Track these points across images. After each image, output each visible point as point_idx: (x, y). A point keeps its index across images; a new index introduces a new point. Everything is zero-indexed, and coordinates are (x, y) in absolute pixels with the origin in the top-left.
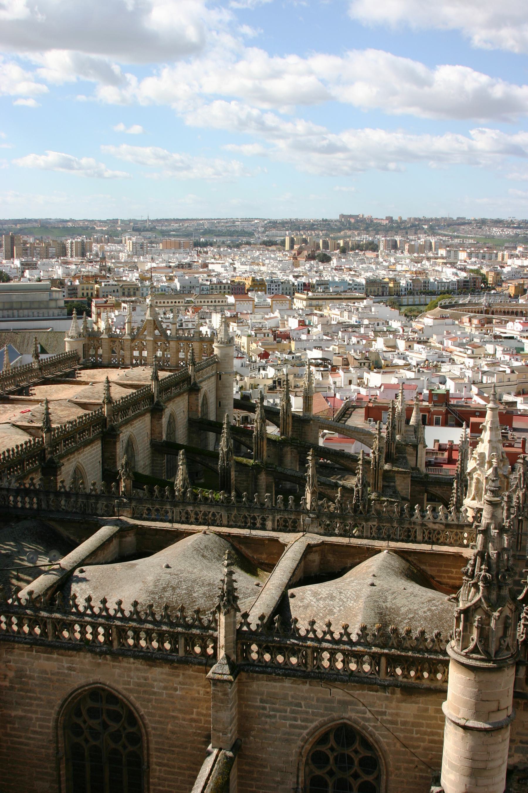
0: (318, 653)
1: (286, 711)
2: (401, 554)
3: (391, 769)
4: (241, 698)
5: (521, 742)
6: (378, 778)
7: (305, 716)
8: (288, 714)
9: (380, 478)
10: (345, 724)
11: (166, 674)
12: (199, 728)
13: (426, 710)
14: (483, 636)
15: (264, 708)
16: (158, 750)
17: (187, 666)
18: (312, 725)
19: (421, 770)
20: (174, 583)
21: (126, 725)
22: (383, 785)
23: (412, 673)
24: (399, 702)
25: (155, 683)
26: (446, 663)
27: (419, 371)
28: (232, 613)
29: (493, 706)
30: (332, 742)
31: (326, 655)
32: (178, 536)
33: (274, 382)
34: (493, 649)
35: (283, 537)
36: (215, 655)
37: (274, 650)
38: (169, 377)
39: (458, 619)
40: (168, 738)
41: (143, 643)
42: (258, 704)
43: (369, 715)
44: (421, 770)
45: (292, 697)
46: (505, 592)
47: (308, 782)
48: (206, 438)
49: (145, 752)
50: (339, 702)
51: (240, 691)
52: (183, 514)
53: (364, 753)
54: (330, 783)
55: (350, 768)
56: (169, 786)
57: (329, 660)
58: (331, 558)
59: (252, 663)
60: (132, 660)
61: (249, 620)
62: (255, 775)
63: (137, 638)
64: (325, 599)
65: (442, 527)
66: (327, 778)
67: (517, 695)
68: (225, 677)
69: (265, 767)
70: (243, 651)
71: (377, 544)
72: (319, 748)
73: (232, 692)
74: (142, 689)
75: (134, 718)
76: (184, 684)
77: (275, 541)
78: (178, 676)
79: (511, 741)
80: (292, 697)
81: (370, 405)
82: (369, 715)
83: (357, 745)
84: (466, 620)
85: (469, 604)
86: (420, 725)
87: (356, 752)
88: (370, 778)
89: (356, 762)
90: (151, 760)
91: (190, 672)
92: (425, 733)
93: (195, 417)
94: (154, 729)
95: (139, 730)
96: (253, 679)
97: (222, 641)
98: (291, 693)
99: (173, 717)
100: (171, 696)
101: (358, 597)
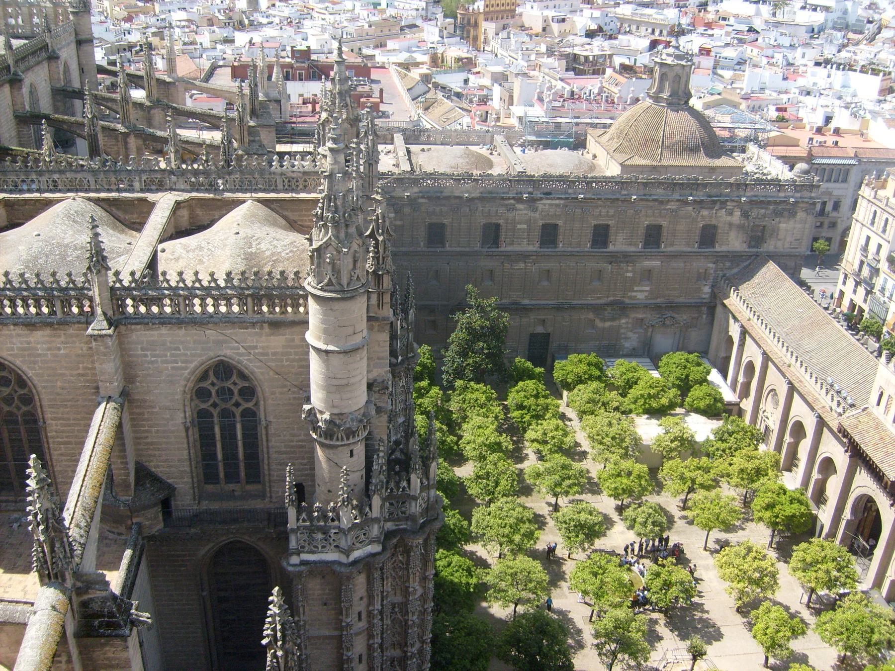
0: (189, 300)
1: (166, 356)
2: (265, 202)
3: (267, 394)
4: (122, 349)
5: (378, 358)
6: (257, 404)
7: (183, 358)
8: (169, 358)
9: (246, 133)
10: (222, 362)
11: (47, 336)
12: (87, 381)
13: (293, 340)
14: (336, 271)
15: (146, 356)
16: (51, 406)
17: (66, 327)
18: (192, 366)
19: (294, 393)
20: (47, 250)
21: (17, 388)
22: (262, 408)
23: (277, 309)
24: (267, 336)
25: (39, 346)
26: (305, 298)
27: (281, 28)
28: (103, 271)
29: (350, 330)
30: (212, 378)
31: (197, 301)
32: (49, 203)
33: (141, 46)
34: (345, 281)
35: (151, 197)
36: (93, 313)
37: (149, 302)
38: (25, 45)
39: (312, 257)
40: (59, 394)
41: (20, 310)
42: (140, 352)
43: (242, 350)
44: (294, 393)
45: (171, 343)
46: (352, 230)
47: (195, 416)
48: (73, 105)
49: (39, 410)
50: (214, 342)
51: (121, 343)
52: (50, 182)
53: (242, 384)
54: (215, 412)
55: (231, 398)
56: (67, 437)
57: (201, 305)
58: (199, 212)
59: (128, 317)
60: (12, 327)
61: (121, 277)
62: (146, 416)
63: (14, 305)
64: (194, 251)
65: (300, 175)
66: (212, 409)
67: (370, 319)
68: (104, 332)
69: (154, 407)
70: (119, 306)
71: (240, 195)
72: (201, 385)
73: (113, 345)
74: (26, 353)
75: (24, 381)
76: (66, 343)
77: (144, 200)
78: (60, 336)
79: (368, 359)
80: (171, 343)
81: (236, 64)
82: (242, 350)
83: (234, 378)
84: (319, 257)
85: (321, 243)
86: (290, 354)
87: (235, 384)
88: (250, 405)
89: (236, 392)
90: (46, 416)
91: (71, 331)
92: (294, 360)
93: (58, 86)
94: (44, 387)
95: (30, 391)
96: (132, 330)
97: (97, 300)
98: (169, 339)
99: (61, 374)
100: (55, 356)
101: (225, 245)
